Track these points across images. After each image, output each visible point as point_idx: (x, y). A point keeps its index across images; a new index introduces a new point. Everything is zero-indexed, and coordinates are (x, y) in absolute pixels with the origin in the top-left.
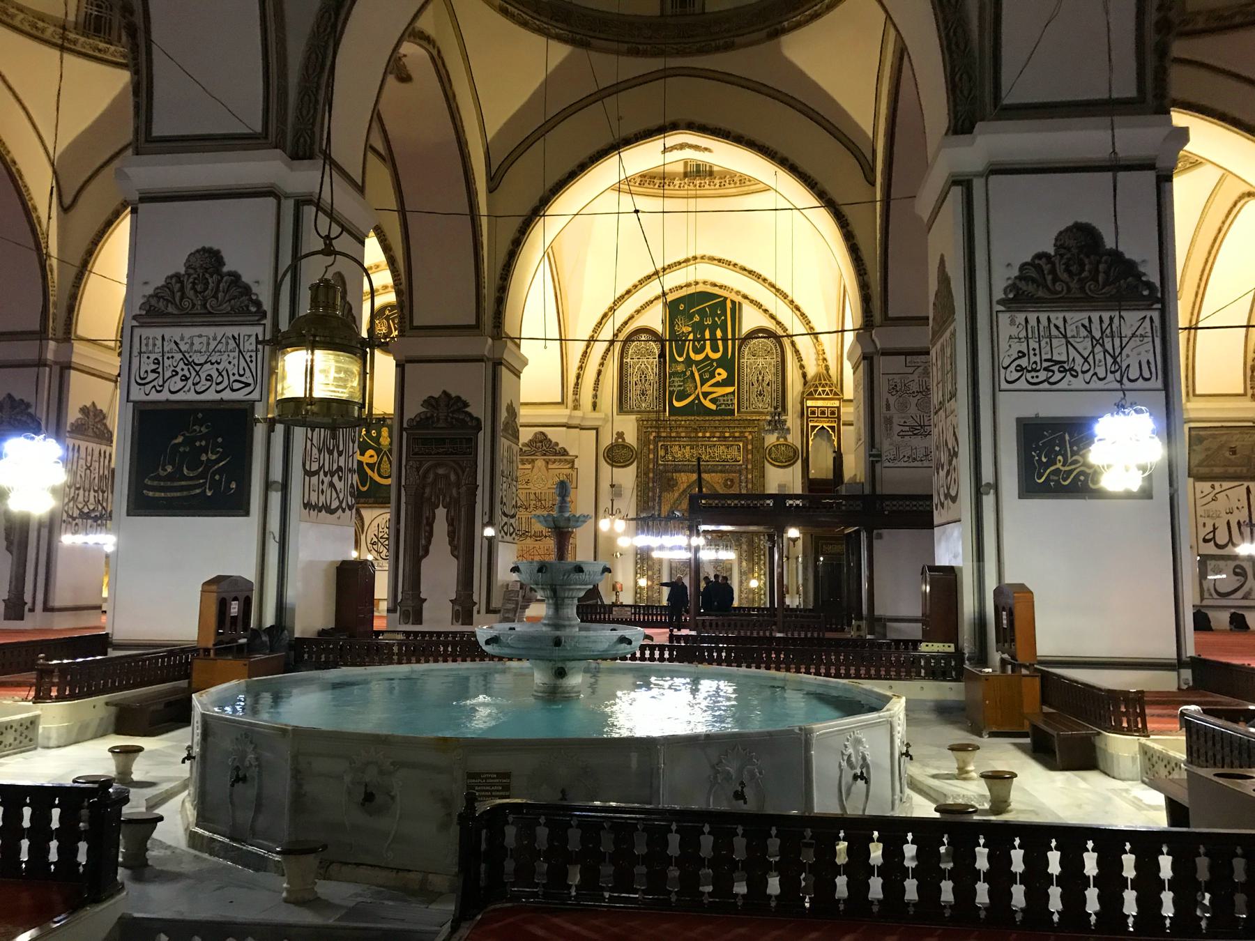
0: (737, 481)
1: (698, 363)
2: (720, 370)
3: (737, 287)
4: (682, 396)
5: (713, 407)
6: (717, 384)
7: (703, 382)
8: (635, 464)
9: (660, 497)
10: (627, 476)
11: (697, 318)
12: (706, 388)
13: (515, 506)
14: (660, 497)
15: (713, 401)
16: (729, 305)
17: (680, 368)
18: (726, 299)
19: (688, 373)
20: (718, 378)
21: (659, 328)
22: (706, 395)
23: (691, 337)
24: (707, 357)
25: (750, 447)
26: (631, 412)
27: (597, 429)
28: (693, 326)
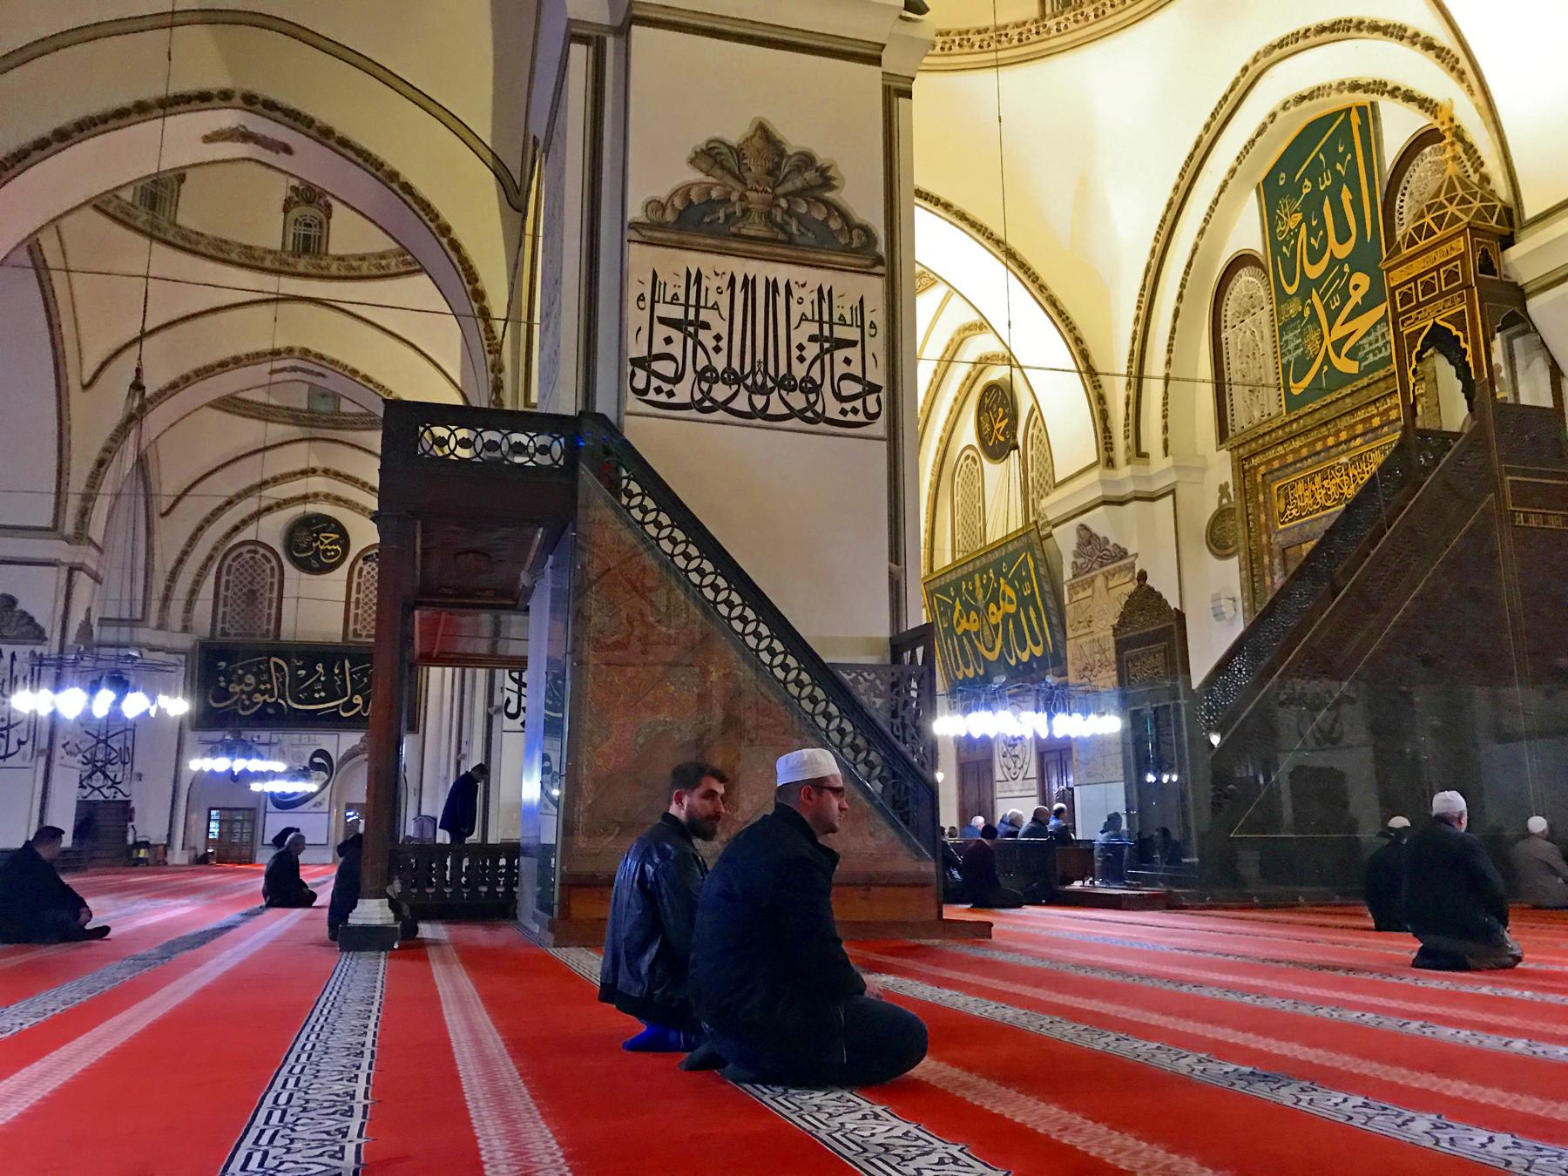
1: (1317, 283)
3: (1334, 77)
5: (1352, 367)
6: (1357, 312)
15: (1351, 355)
16: (1355, 120)
17: (1293, 308)
19: (1307, 313)
22: (1338, 345)
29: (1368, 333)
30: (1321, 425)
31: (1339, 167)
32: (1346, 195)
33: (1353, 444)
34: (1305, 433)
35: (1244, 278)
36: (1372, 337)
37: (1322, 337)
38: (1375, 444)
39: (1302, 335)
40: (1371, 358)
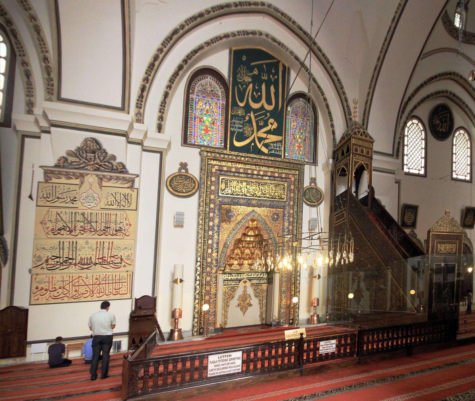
0: (281, 215)
1: (255, 111)
2: (271, 120)
4: (241, 137)
6: (268, 132)
7: (259, 128)
8: (197, 195)
9: (219, 226)
10: (190, 206)
11: (256, 72)
12: (261, 134)
13: (58, 230)
14: (219, 226)
15: (266, 146)
17: (240, 112)
18: (279, 62)
19: (247, 118)
20: (269, 127)
21: (224, 70)
22: (260, 139)
23: (251, 86)
24: (262, 108)
25: (292, 187)
26: (193, 145)
27: (161, 153)
28: (253, 77)
29: (273, 143)
30: (254, 165)
31: (271, 76)
32: (272, 89)
33: (264, 178)
34: (245, 164)
35: (209, 80)
36: (275, 145)
37: (253, 131)
38: (273, 182)
39: (243, 124)
40: (273, 152)
